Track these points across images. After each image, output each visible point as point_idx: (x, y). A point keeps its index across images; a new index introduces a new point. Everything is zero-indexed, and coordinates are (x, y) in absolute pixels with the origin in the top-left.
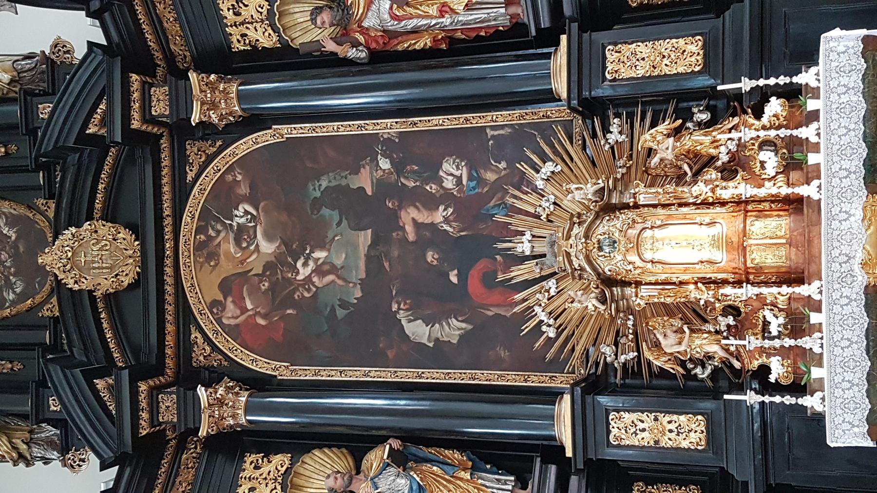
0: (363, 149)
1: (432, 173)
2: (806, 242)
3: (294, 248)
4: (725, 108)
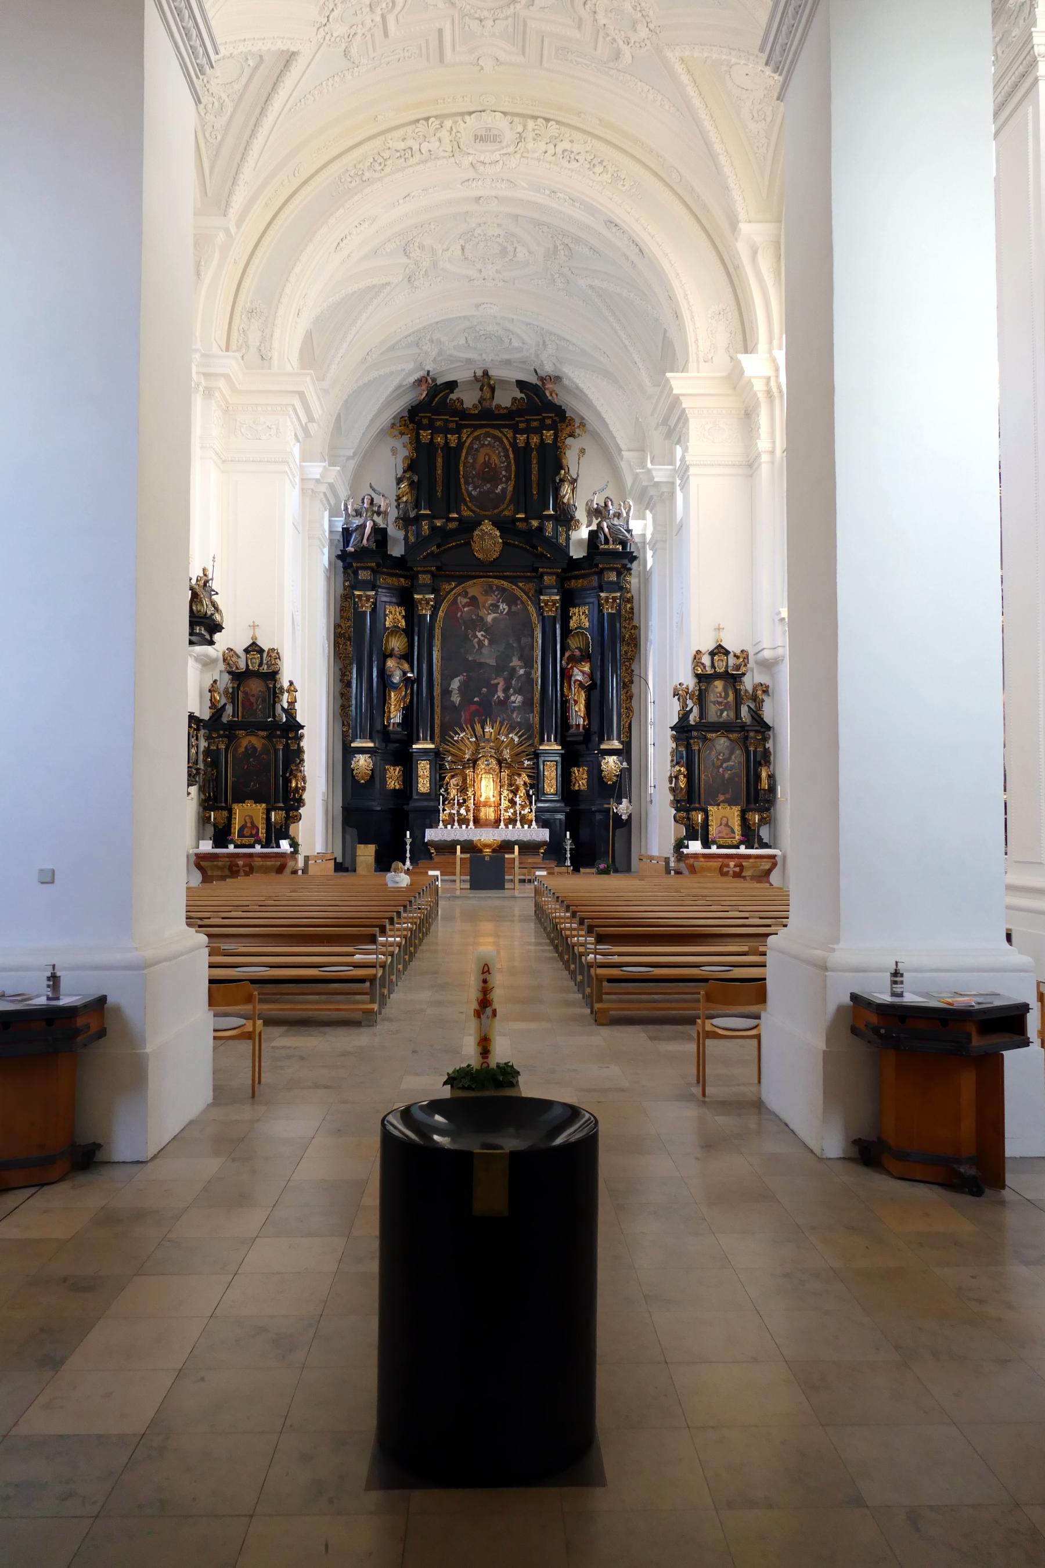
0: (529, 663)
1: (519, 691)
3: (488, 630)
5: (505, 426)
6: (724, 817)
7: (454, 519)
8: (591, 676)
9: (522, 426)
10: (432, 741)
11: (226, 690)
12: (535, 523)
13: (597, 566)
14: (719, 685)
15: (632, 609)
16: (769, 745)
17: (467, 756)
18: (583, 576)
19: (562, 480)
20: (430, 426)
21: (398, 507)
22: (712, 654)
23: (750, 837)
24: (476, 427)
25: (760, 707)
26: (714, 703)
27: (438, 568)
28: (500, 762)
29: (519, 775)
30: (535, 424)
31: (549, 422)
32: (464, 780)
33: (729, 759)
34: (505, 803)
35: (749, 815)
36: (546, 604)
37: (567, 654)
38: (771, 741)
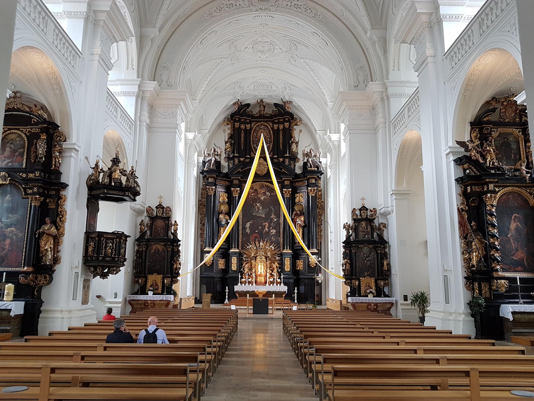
2: (261, 284)
3: (262, 203)
4: (279, 274)
5: (269, 121)
6: (367, 282)
7: (248, 158)
8: (304, 222)
9: (276, 121)
10: (238, 248)
11: (147, 224)
12: (281, 160)
13: (307, 176)
14: (364, 223)
15: (321, 194)
16: (387, 250)
17: (252, 255)
18: (301, 181)
19: (292, 142)
20: (239, 121)
21: (225, 153)
22: (360, 210)
23: (379, 293)
24: (258, 122)
25: (382, 234)
26: (361, 231)
27: (242, 178)
28: (266, 258)
29: (274, 263)
30: (282, 120)
31: (287, 119)
32: (251, 265)
33: (369, 257)
34: (268, 275)
35: (379, 282)
36: (286, 193)
37: (294, 213)
38: (387, 248)
